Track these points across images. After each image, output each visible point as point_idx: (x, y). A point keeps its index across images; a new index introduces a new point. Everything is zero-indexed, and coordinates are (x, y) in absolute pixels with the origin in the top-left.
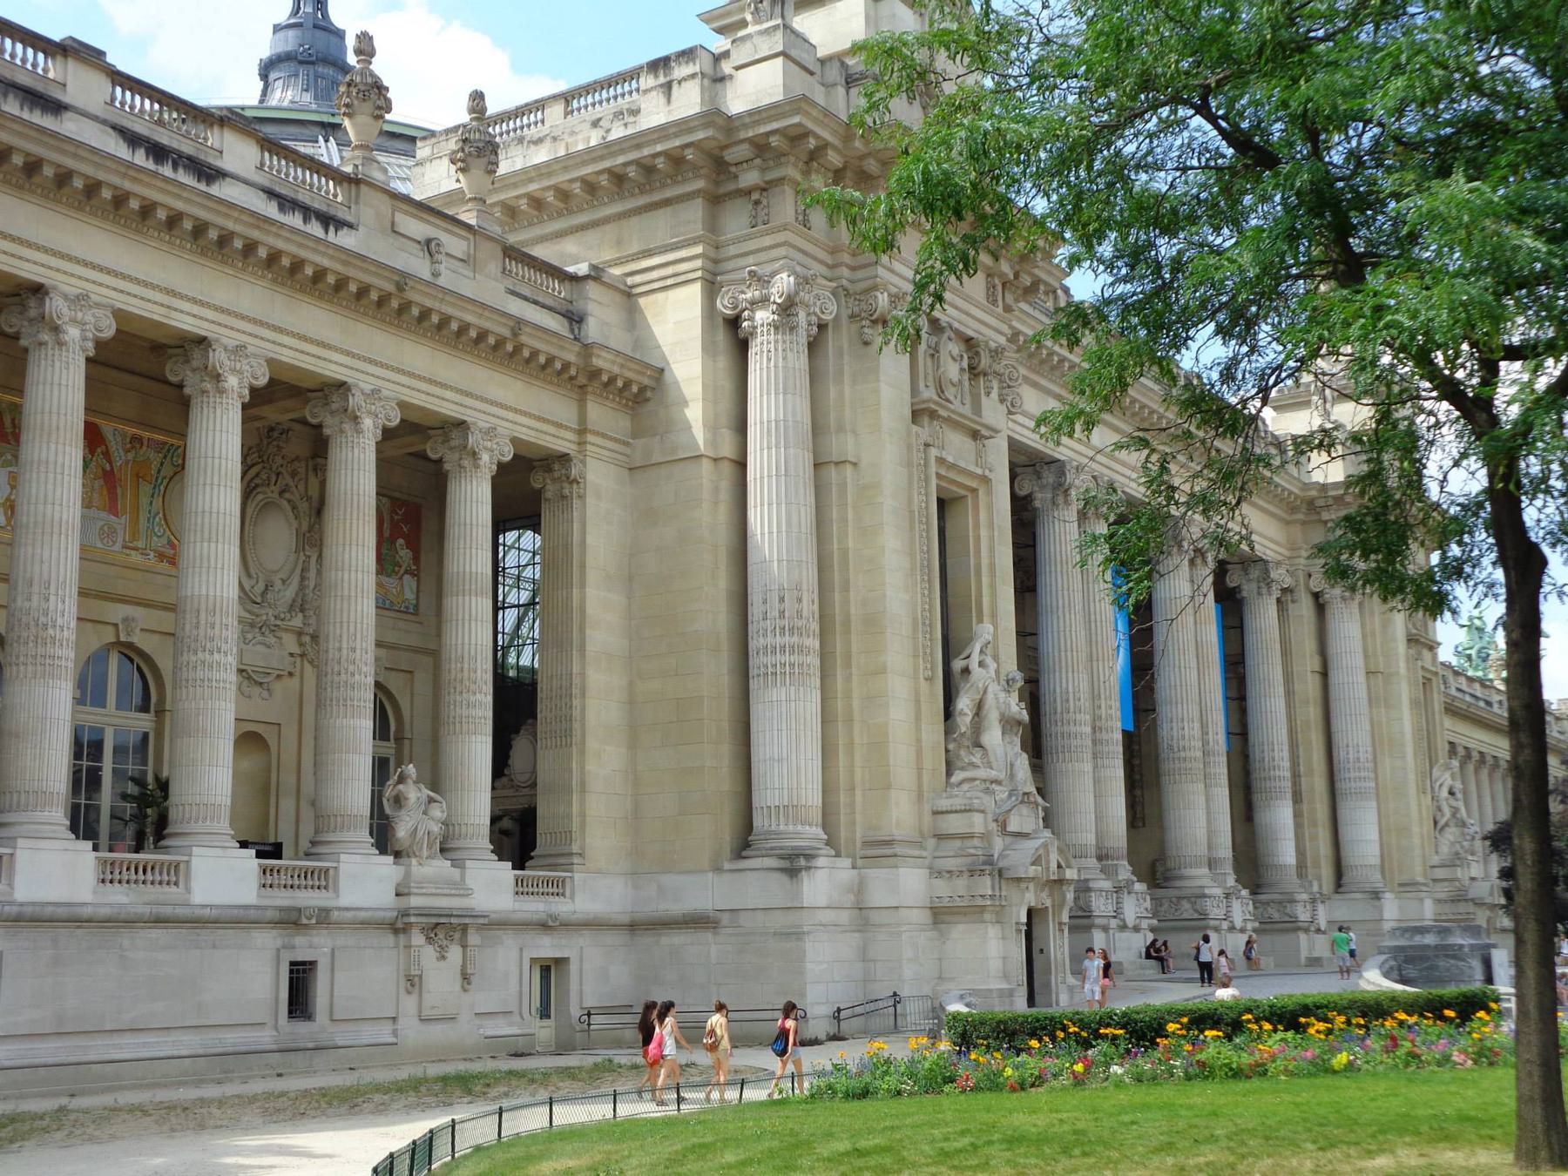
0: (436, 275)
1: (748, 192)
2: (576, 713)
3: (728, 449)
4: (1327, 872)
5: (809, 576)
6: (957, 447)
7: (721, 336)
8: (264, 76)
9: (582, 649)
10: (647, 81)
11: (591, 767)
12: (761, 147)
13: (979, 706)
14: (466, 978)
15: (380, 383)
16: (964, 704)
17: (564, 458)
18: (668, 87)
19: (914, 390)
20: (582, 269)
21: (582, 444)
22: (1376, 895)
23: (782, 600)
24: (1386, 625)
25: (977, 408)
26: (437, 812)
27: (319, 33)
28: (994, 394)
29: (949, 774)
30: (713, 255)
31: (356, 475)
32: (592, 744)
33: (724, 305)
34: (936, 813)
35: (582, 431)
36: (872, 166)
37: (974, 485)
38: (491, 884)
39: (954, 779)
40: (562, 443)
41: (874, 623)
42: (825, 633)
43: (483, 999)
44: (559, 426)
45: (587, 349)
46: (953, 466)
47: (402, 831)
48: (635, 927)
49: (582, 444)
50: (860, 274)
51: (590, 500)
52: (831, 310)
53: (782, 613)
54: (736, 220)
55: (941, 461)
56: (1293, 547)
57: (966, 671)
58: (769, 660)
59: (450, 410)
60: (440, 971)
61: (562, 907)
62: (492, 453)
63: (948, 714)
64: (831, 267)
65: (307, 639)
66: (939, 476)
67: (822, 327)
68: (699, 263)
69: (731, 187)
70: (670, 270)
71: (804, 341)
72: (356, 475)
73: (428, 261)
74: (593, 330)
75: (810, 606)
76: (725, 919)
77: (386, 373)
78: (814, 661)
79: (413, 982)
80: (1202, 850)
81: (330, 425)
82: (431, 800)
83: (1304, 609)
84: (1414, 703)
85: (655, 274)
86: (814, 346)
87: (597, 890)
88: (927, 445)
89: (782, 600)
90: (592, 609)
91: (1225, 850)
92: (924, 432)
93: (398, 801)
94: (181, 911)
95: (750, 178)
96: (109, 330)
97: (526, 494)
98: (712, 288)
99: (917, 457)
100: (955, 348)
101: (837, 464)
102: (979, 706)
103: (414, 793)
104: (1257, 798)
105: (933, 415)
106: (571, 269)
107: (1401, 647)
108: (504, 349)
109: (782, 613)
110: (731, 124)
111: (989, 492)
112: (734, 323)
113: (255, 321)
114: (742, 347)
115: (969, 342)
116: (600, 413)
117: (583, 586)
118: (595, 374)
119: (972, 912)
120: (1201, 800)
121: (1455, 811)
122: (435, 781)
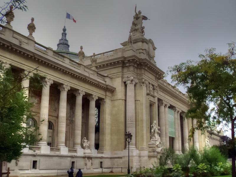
0: (89, 76)
1: (127, 66)
2: (105, 131)
3: (124, 98)
6: (152, 99)
7: (123, 84)
8: (58, 46)
9: (106, 123)
11: (106, 138)
12: (129, 61)
13: (154, 131)
14: (92, 164)
15: (83, 90)
16: (152, 131)
17: (104, 99)
19: (147, 92)
20: (106, 75)
21: (106, 97)
23: (131, 117)
25: (154, 94)
26: (88, 143)
27: (65, 41)
28: (156, 92)
29: (151, 139)
30: (122, 74)
31: (79, 100)
32: (106, 135)
33: (124, 80)
34: (149, 144)
36: (142, 64)
37: (153, 103)
38: (93, 152)
39: (152, 140)
40: (103, 97)
41: (142, 120)
43: (94, 166)
44: (103, 95)
46: (151, 101)
47: (84, 145)
48: (111, 158)
49: (106, 97)
50: (141, 77)
51: (107, 104)
53: (131, 119)
54: (125, 70)
55: (150, 100)
57: (153, 127)
58: (129, 125)
59: (91, 93)
60: (89, 163)
61: (103, 155)
64: (137, 76)
65: (71, 121)
66: (150, 102)
67: (136, 83)
68: (121, 75)
69: (125, 66)
70: (117, 76)
71: (133, 85)
72: (79, 100)
73: (88, 74)
75: (134, 118)
76: (123, 157)
77: (83, 88)
78: (135, 125)
79: (86, 164)
80: (178, 149)
81: (90, 99)
82: (88, 142)
85: (115, 76)
86: (135, 86)
87: (107, 153)
88: (148, 98)
89: (131, 117)
90: (107, 118)
91: (181, 149)
92: (148, 97)
93: (84, 142)
94: (60, 155)
95: (128, 65)
96: (52, 82)
97: (99, 104)
98: (122, 78)
99: (147, 100)
100: (151, 86)
101: (137, 100)
102: (154, 131)
103: (86, 141)
104: (184, 142)
105: (149, 95)
106: (105, 75)
108: (97, 85)
109: (131, 119)
110: (125, 58)
111: (155, 104)
112: (125, 83)
113: (88, 89)
114: (126, 86)
115: (153, 85)
116: (108, 94)
117: (106, 115)
119: (154, 157)
120: (178, 143)
121: (208, 144)
122: (88, 139)
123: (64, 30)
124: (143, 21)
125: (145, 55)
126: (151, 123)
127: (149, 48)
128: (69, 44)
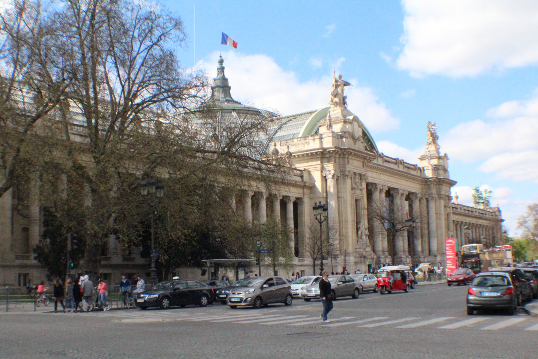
4: (427, 252)
5: (337, 215)
7: (324, 178)
10: (310, 138)
12: (329, 152)
16: (360, 232)
17: (301, 198)
18: (314, 139)
21: (304, 196)
22: (436, 256)
24: (440, 203)
33: (324, 175)
35: (304, 194)
40: (300, 196)
41: (346, 221)
42: (340, 224)
45: (305, 183)
52: (339, 175)
56: (422, 189)
62: (293, 199)
63: (357, 233)
74: (304, 178)
75: (337, 220)
83: (424, 201)
84: (445, 219)
86: (337, 180)
107: (443, 208)
112: (325, 177)
114: (326, 180)
115: (360, 175)
118: (305, 186)
123: (221, 62)
124: (345, 87)
125: (349, 138)
126: (358, 223)
127: (353, 129)
128: (230, 85)
